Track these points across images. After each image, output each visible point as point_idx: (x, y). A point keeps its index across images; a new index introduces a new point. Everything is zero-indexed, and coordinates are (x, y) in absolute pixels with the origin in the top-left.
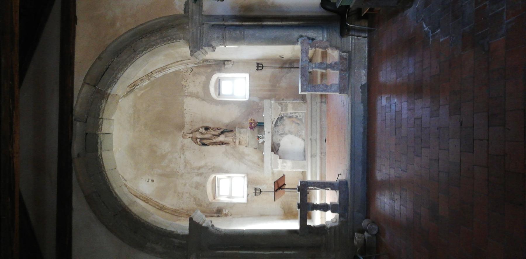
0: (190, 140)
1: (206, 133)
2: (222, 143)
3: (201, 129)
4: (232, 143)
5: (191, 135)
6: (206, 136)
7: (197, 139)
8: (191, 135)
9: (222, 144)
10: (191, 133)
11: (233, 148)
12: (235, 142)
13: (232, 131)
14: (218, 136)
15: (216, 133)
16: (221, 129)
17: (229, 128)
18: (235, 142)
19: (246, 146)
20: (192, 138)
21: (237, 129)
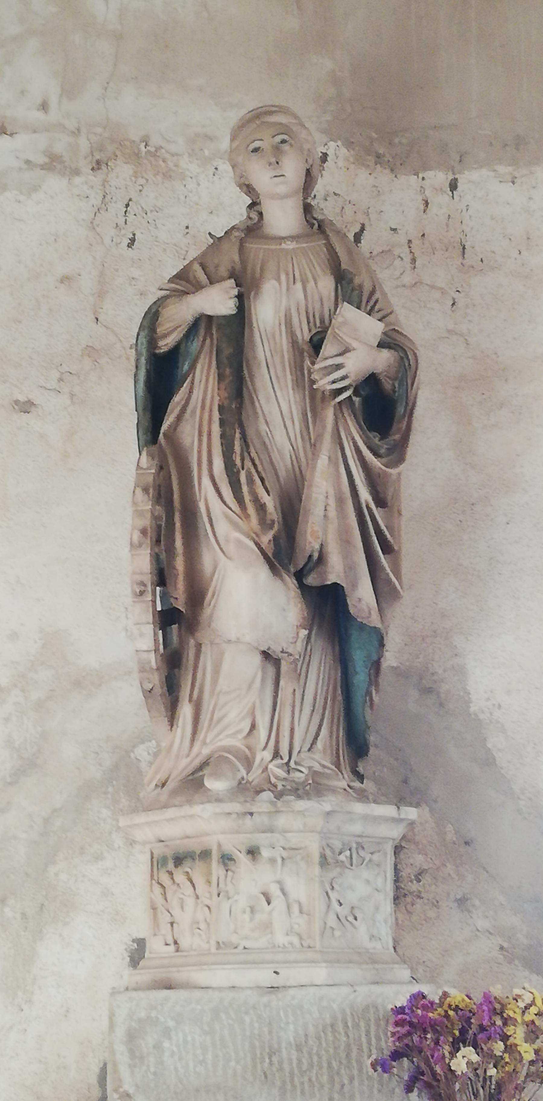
0: (235, 210)
1: (314, 400)
2: (179, 618)
3: (373, 328)
4: (175, 749)
5: (283, 218)
6: (277, 406)
7: (246, 287)
8: (283, 218)
9: (167, 618)
10: (315, 224)
11: (123, 782)
12: (193, 783)
13: (355, 744)
14: (284, 553)
15: (326, 526)
16: (384, 590)
17: (388, 705)
18: (193, 783)
19: (137, 954)
20: (253, 229)
21: (380, 820)
